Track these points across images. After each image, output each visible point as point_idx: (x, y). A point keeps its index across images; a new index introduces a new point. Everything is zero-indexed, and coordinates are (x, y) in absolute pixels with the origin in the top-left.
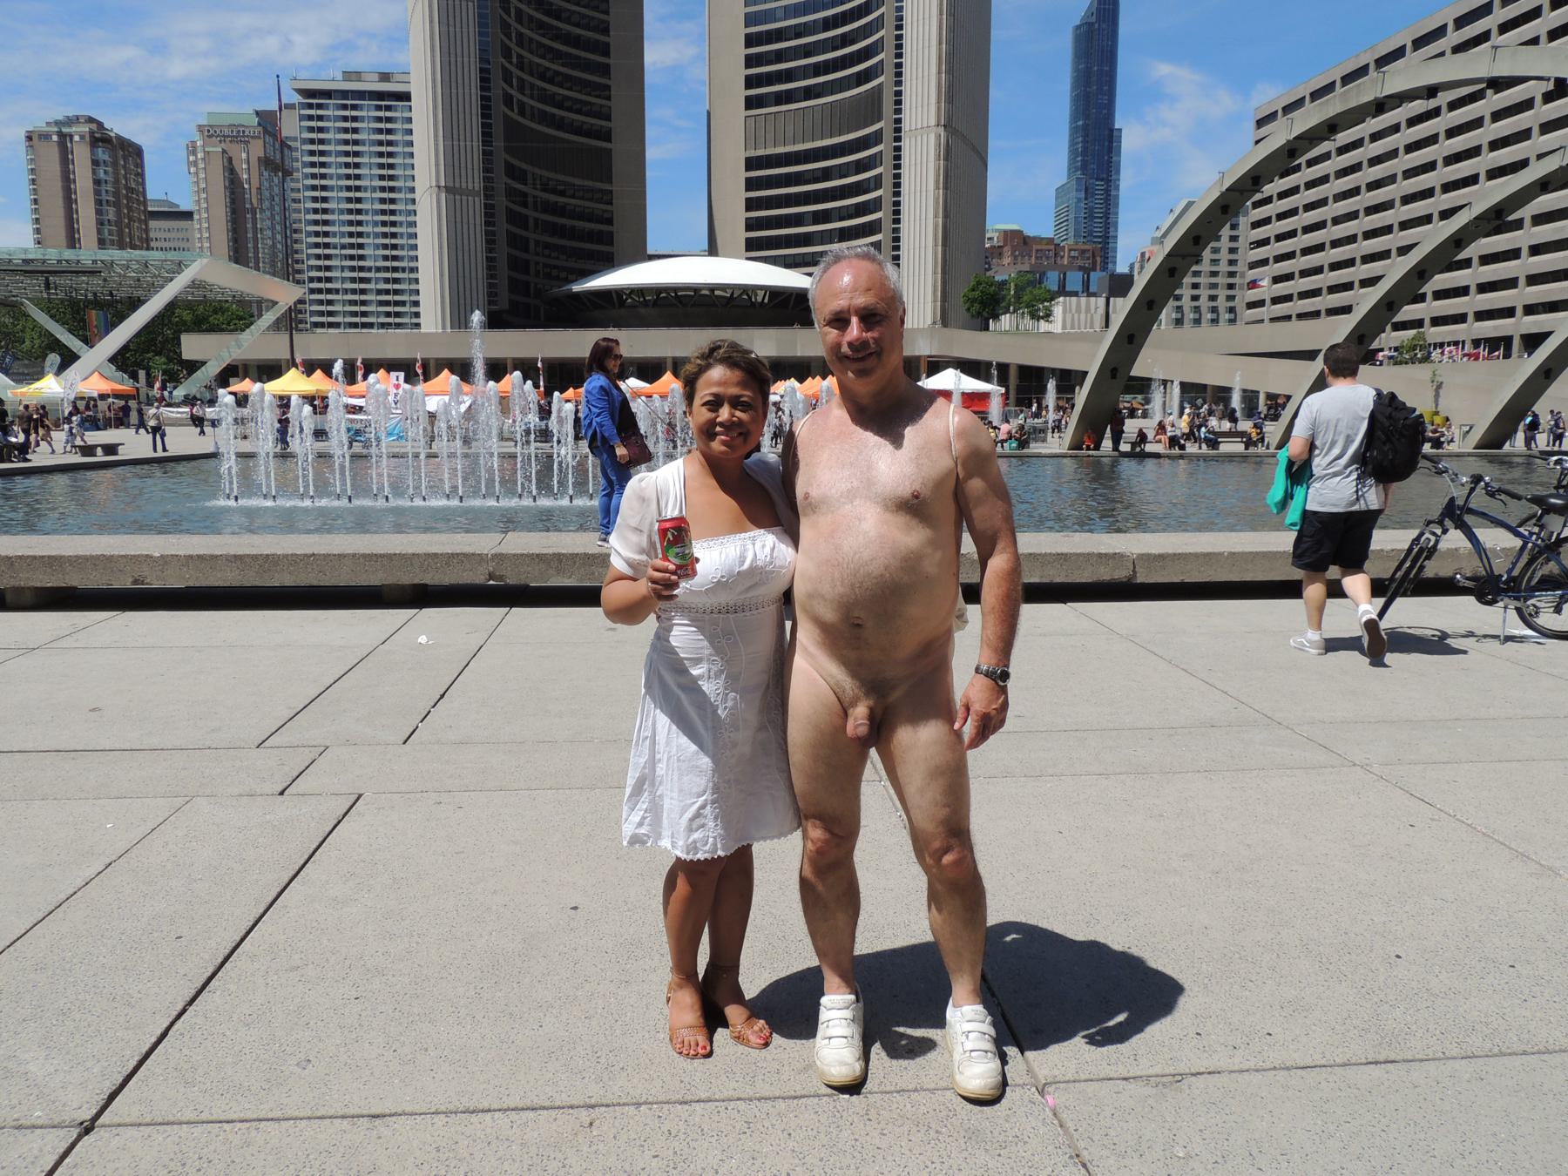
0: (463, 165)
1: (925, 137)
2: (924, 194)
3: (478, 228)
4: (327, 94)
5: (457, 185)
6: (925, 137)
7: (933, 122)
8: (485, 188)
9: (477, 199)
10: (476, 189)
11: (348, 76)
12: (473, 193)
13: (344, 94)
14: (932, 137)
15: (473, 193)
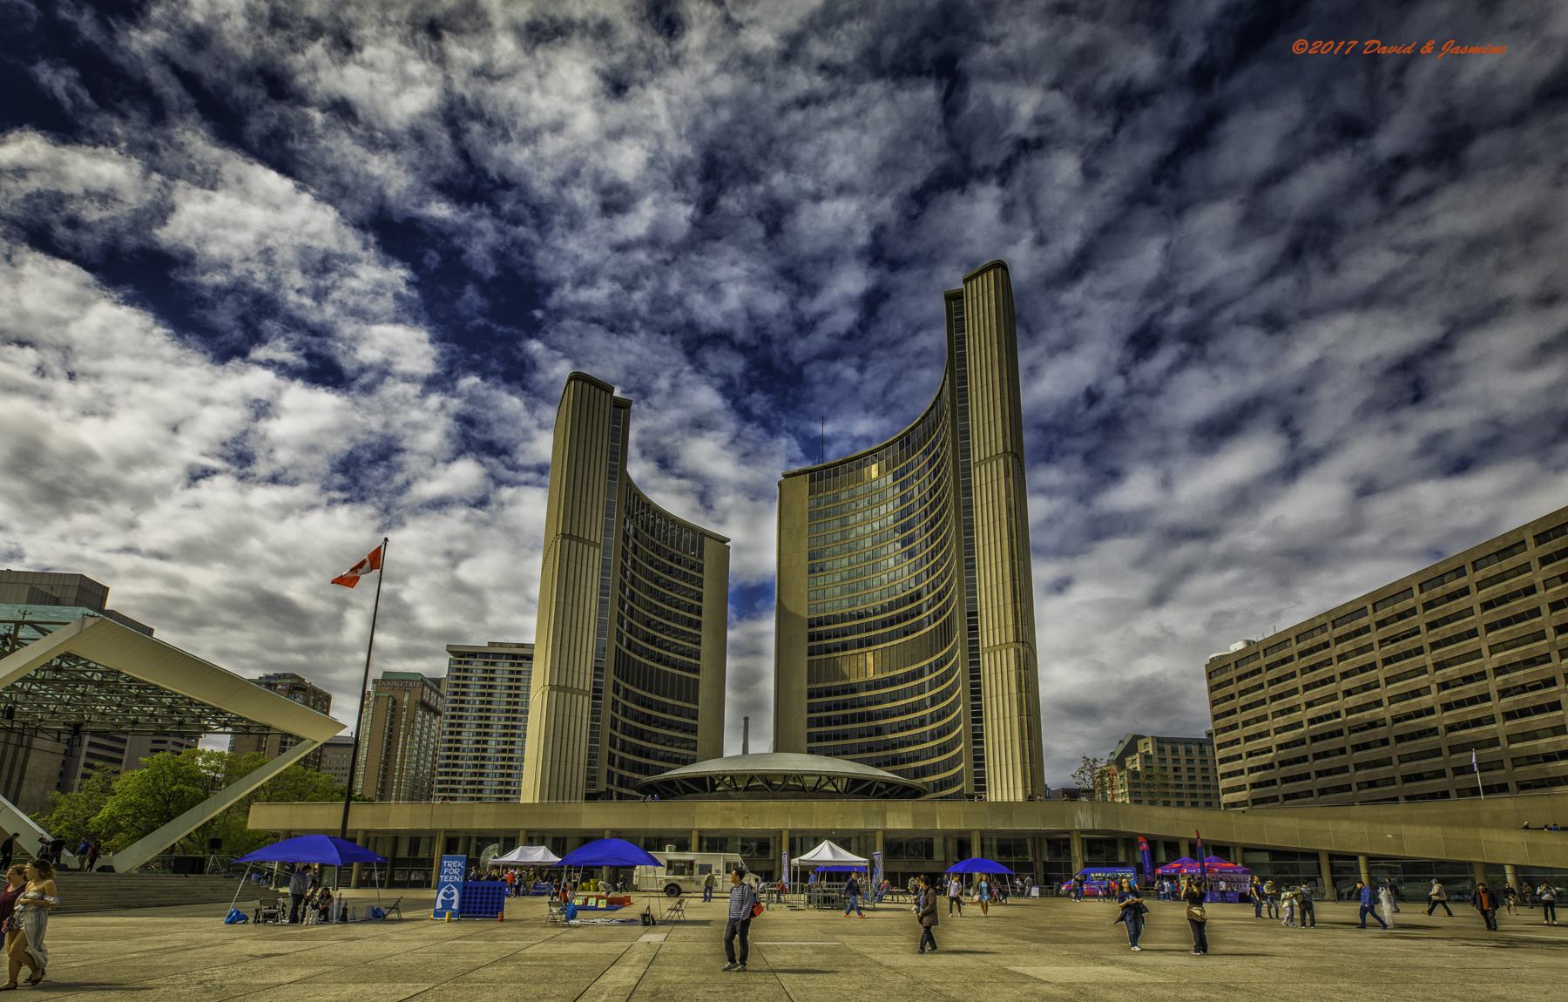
0: (576, 669)
1: (1004, 652)
2: (1007, 697)
3: (585, 722)
4: (474, 655)
5: (569, 685)
6: (1004, 652)
7: (1011, 639)
8: (595, 690)
9: (586, 698)
10: (587, 689)
11: (492, 644)
12: (584, 692)
13: (486, 655)
14: (1012, 651)
15: (584, 692)
